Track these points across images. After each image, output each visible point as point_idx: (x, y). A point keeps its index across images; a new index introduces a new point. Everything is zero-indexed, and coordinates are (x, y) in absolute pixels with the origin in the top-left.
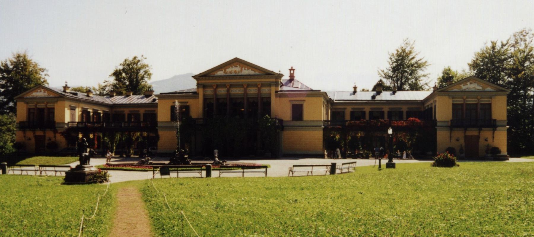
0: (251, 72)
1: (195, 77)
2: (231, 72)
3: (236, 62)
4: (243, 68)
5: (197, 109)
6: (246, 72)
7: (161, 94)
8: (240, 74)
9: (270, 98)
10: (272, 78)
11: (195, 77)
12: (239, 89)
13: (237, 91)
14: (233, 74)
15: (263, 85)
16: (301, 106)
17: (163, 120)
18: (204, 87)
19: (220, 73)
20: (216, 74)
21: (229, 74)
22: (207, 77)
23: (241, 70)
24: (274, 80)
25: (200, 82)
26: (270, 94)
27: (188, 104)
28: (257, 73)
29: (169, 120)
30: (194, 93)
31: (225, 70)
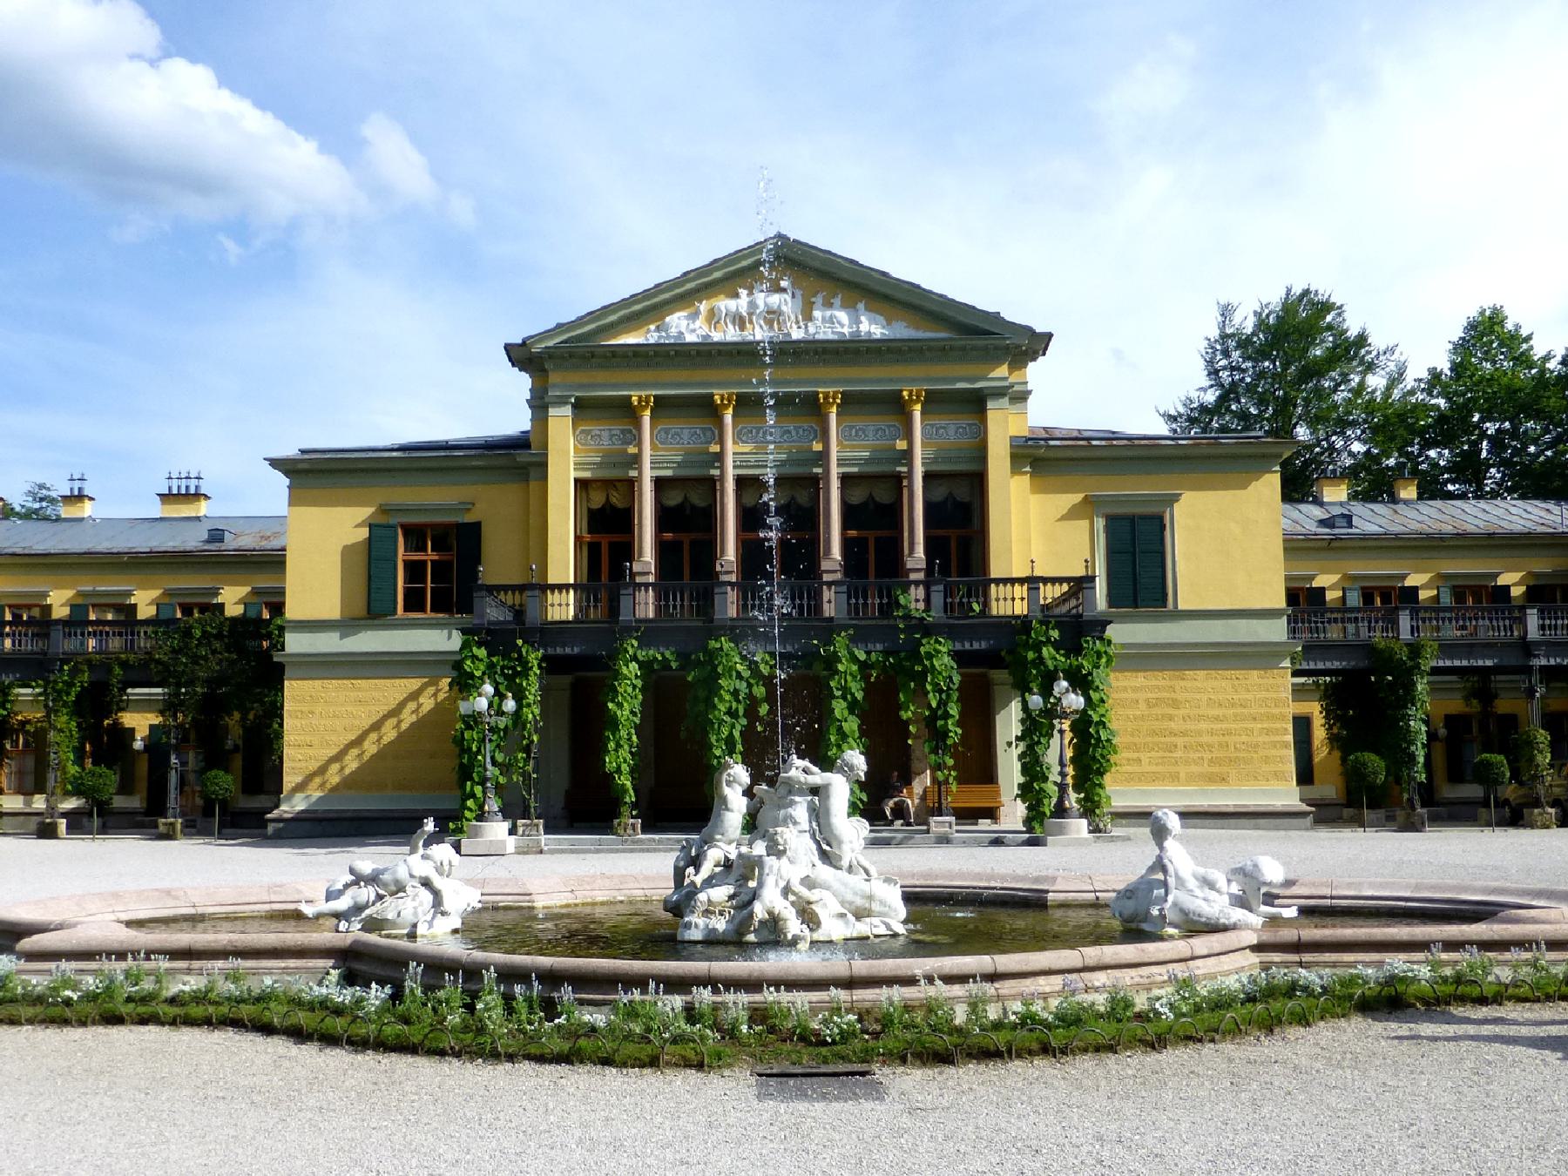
0: (872, 327)
1: (521, 356)
4: (819, 299)
6: (837, 322)
9: (978, 480)
19: (684, 327)
27: (468, 518)
28: (902, 330)
30: (519, 443)
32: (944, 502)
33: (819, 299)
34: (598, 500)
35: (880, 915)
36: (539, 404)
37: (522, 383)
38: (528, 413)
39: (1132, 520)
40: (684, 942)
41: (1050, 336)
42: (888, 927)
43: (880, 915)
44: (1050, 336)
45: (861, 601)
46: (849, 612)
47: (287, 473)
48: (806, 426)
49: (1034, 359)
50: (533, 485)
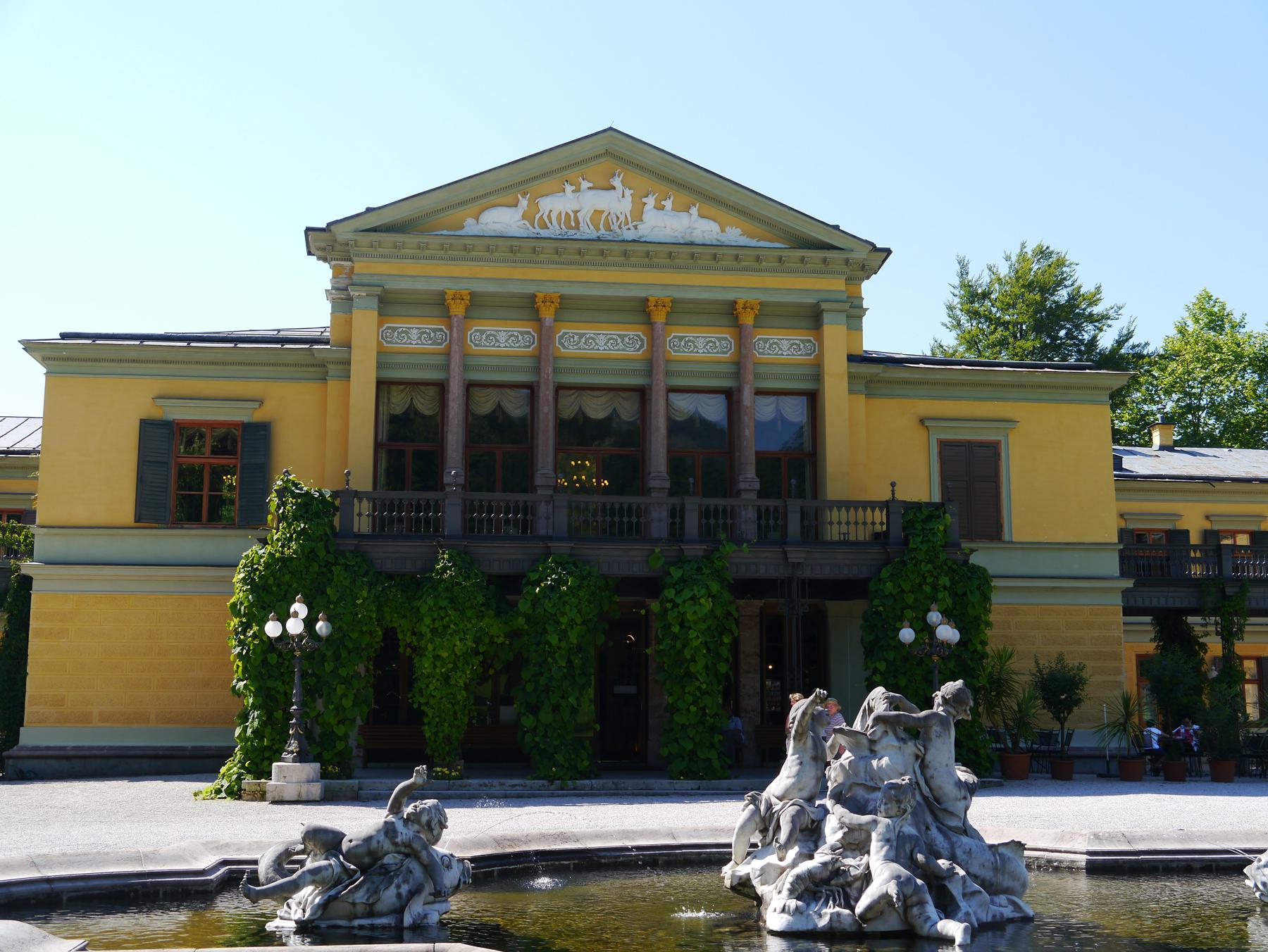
0: (703, 228)
1: (322, 241)
2: (572, 220)
3: (611, 154)
4: (650, 201)
5: (323, 446)
6: (667, 222)
7: (64, 336)
8: (630, 235)
9: (813, 399)
10: (825, 269)
11: (322, 241)
12: (614, 332)
13: (601, 346)
14: (587, 231)
15: (770, 314)
16: (991, 453)
17: (80, 515)
18: (389, 303)
19: (503, 220)
20: (471, 227)
21: (554, 230)
22: (410, 240)
23: (638, 214)
24: (837, 284)
25: (360, 266)
26: (817, 374)
27: (258, 416)
28: (734, 235)
29: (126, 512)
31: (533, 204)
32: (774, 421)
33: (650, 201)
34: (398, 402)
35: (1007, 891)
36: (342, 298)
37: (321, 274)
38: (327, 307)
39: (969, 446)
40: (921, 938)
41: (888, 252)
42: (1017, 907)
43: (1007, 891)
44: (888, 252)
45: (625, 519)
46: (802, 534)
47: (44, 360)
48: (631, 333)
49: (868, 278)
50: (332, 384)
